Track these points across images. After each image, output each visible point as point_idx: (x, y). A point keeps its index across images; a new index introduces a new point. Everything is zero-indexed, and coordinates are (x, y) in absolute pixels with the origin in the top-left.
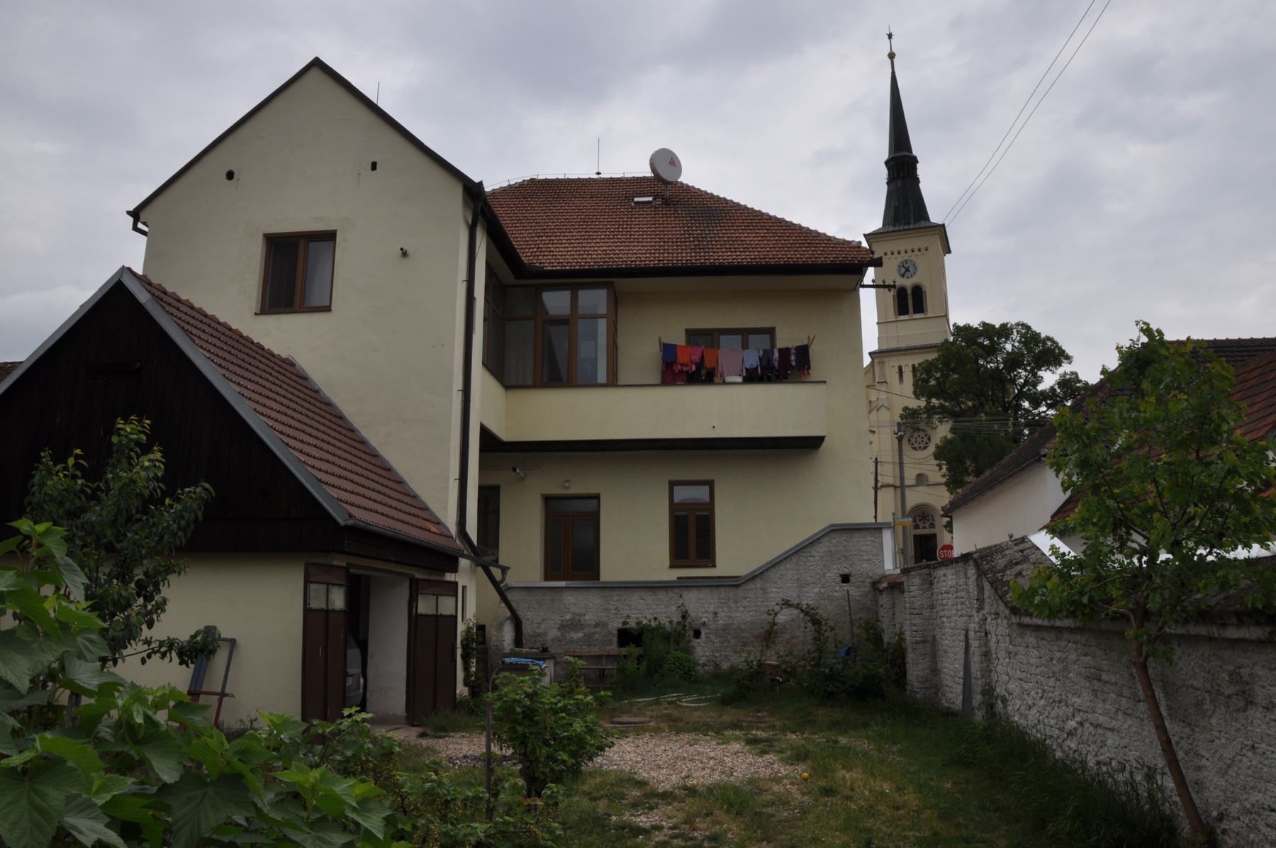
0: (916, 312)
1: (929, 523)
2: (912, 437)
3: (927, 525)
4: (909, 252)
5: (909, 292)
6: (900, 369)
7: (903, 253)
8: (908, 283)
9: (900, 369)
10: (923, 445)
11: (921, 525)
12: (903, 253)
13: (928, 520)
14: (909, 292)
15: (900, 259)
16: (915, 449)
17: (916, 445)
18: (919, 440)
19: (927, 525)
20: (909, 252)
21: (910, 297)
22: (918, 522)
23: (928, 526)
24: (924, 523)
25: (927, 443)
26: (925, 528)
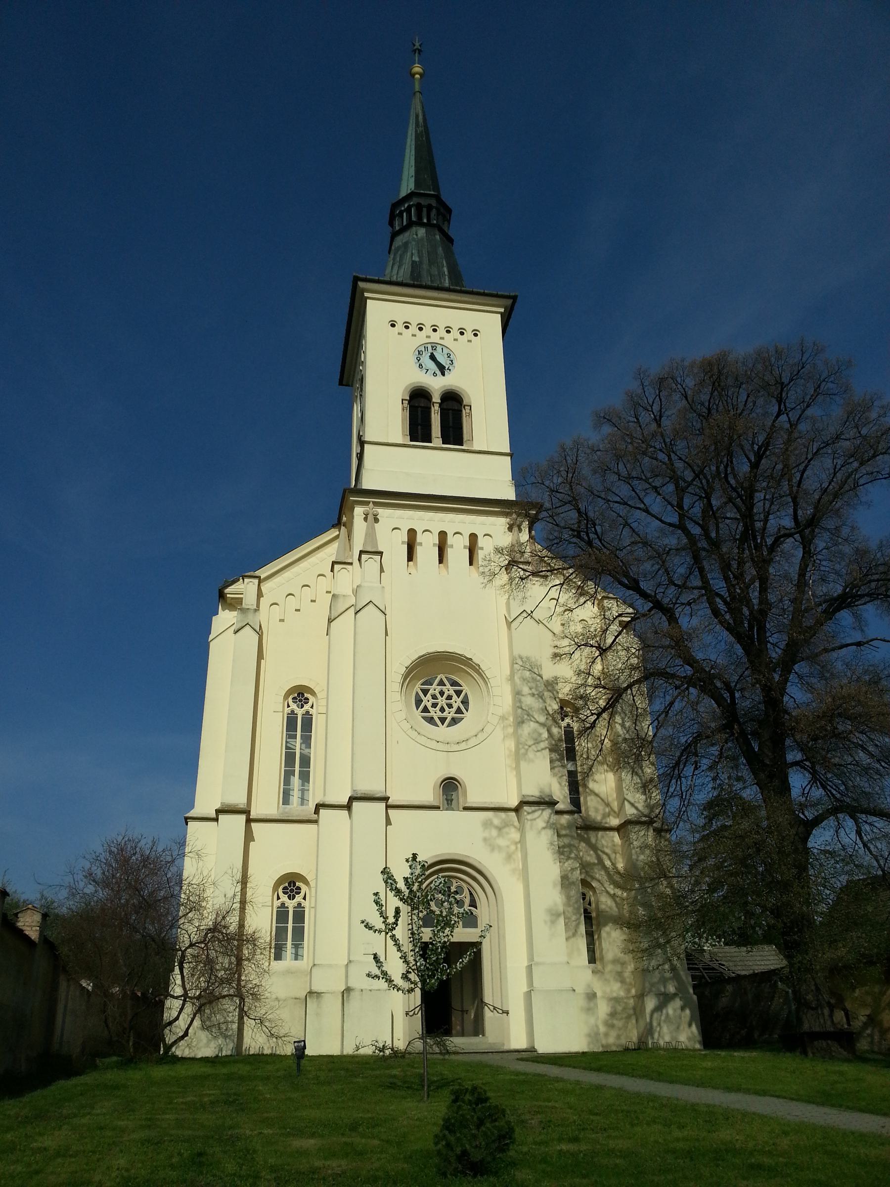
2: (425, 692)
4: (441, 332)
5: (436, 399)
6: (412, 533)
7: (428, 330)
8: (436, 385)
9: (412, 533)
10: (450, 714)
12: (428, 330)
13: (460, 903)
14: (436, 399)
15: (422, 338)
16: (431, 720)
17: (435, 713)
18: (442, 701)
20: (441, 332)
25: (459, 711)
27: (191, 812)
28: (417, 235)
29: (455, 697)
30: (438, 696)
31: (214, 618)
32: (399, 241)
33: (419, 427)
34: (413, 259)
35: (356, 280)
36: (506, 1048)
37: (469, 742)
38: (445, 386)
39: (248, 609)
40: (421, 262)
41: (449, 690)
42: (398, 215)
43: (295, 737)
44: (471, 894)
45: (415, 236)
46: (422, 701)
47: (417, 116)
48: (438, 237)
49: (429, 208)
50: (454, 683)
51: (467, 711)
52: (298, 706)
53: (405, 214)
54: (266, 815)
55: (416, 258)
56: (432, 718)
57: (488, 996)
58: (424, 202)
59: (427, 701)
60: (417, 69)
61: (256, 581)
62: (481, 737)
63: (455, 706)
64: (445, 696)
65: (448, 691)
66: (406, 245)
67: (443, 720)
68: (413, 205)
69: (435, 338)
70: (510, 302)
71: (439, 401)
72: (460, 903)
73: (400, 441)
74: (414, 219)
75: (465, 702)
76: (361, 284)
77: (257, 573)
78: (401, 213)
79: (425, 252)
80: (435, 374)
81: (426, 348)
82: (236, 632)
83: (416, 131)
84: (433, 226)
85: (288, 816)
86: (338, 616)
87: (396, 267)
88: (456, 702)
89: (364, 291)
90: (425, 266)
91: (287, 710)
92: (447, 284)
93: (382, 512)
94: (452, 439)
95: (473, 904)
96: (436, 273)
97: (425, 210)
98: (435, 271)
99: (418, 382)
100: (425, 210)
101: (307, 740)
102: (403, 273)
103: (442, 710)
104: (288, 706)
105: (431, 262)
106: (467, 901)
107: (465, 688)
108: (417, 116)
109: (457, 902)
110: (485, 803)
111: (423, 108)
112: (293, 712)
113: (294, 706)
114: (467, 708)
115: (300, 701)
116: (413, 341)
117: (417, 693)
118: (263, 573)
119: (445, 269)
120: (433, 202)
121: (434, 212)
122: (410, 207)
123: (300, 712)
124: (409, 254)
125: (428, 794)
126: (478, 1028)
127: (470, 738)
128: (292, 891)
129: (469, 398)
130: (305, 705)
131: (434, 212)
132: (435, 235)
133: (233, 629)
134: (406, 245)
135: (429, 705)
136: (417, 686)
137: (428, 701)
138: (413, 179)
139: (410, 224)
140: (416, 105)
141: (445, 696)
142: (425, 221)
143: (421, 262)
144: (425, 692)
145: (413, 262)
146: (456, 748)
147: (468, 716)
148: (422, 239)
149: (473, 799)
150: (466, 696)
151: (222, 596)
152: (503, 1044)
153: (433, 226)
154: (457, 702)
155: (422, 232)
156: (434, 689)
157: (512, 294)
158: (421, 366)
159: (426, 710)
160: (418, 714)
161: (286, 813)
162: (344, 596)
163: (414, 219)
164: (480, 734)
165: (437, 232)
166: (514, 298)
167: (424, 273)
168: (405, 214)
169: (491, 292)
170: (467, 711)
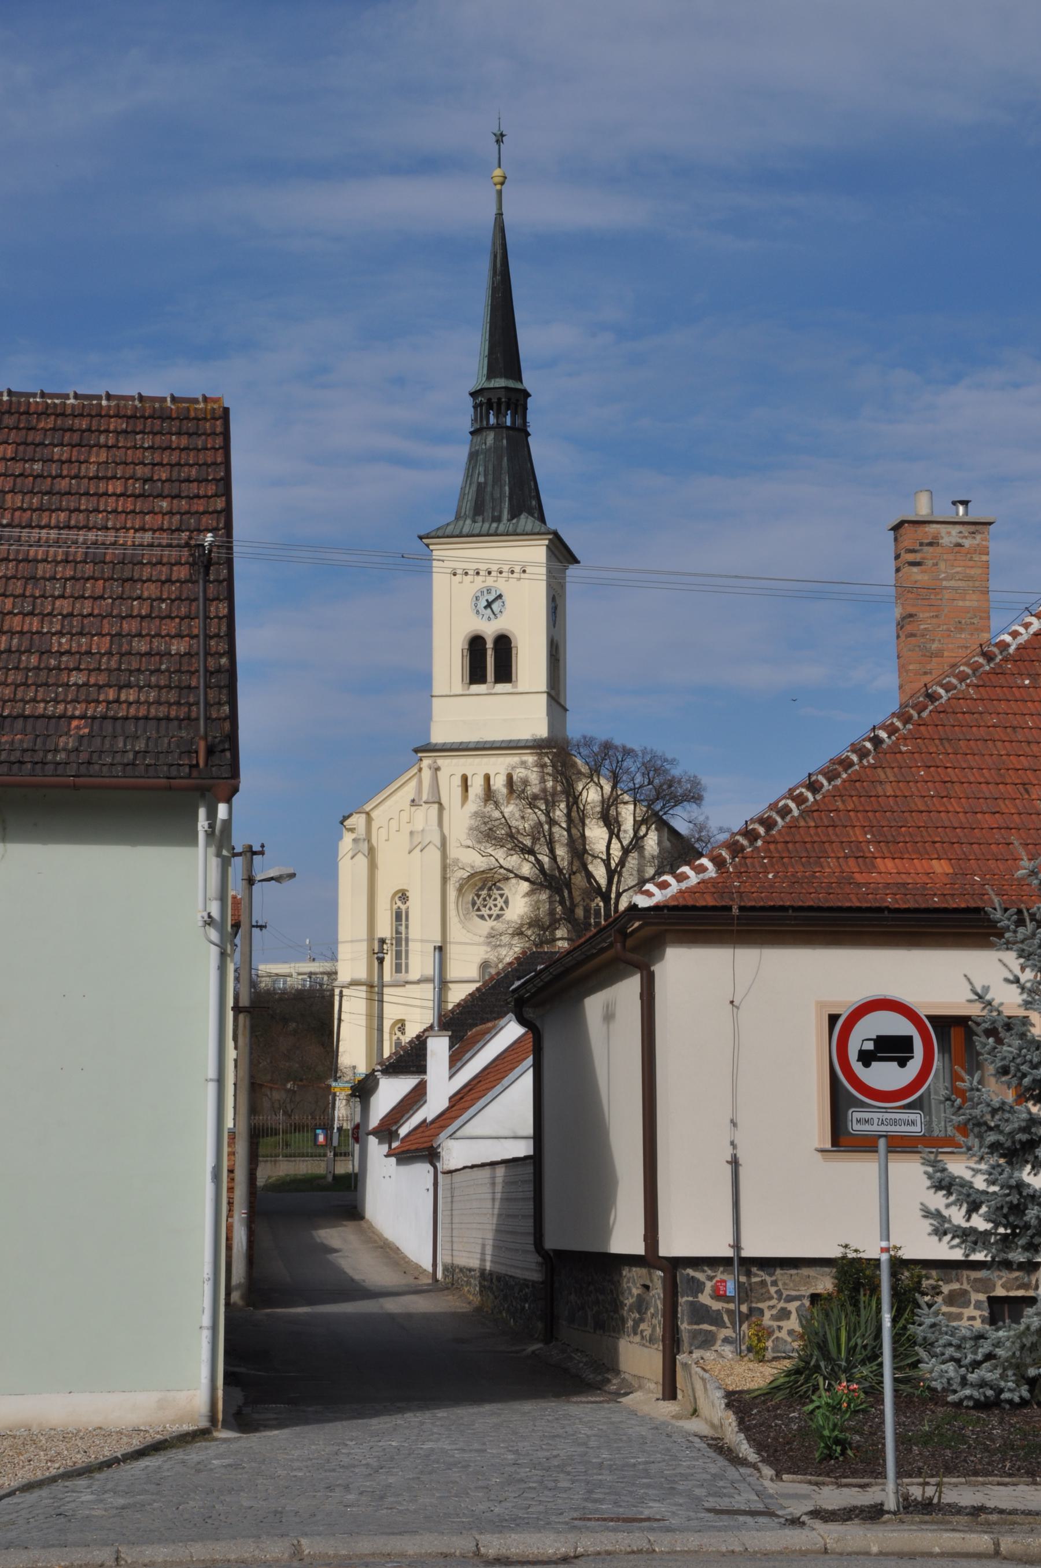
5: (490, 645)
8: (489, 630)
15: (479, 582)
31: (340, 843)
40: (486, 483)
43: (401, 925)
55: (482, 479)
61: (364, 816)
64: (493, 898)
69: (490, 581)
73: (461, 693)
75: (506, 902)
79: (491, 467)
80: (489, 619)
82: (352, 858)
90: (489, 489)
91: (395, 907)
93: (440, 762)
98: (497, 495)
105: (497, 480)
107: (506, 892)
112: (399, 908)
113: (399, 904)
116: (472, 586)
119: (507, 488)
123: (403, 907)
132: (502, 440)
133: (350, 854)
145: (479, 484)
150: (507, 897)
167: (488, 498)
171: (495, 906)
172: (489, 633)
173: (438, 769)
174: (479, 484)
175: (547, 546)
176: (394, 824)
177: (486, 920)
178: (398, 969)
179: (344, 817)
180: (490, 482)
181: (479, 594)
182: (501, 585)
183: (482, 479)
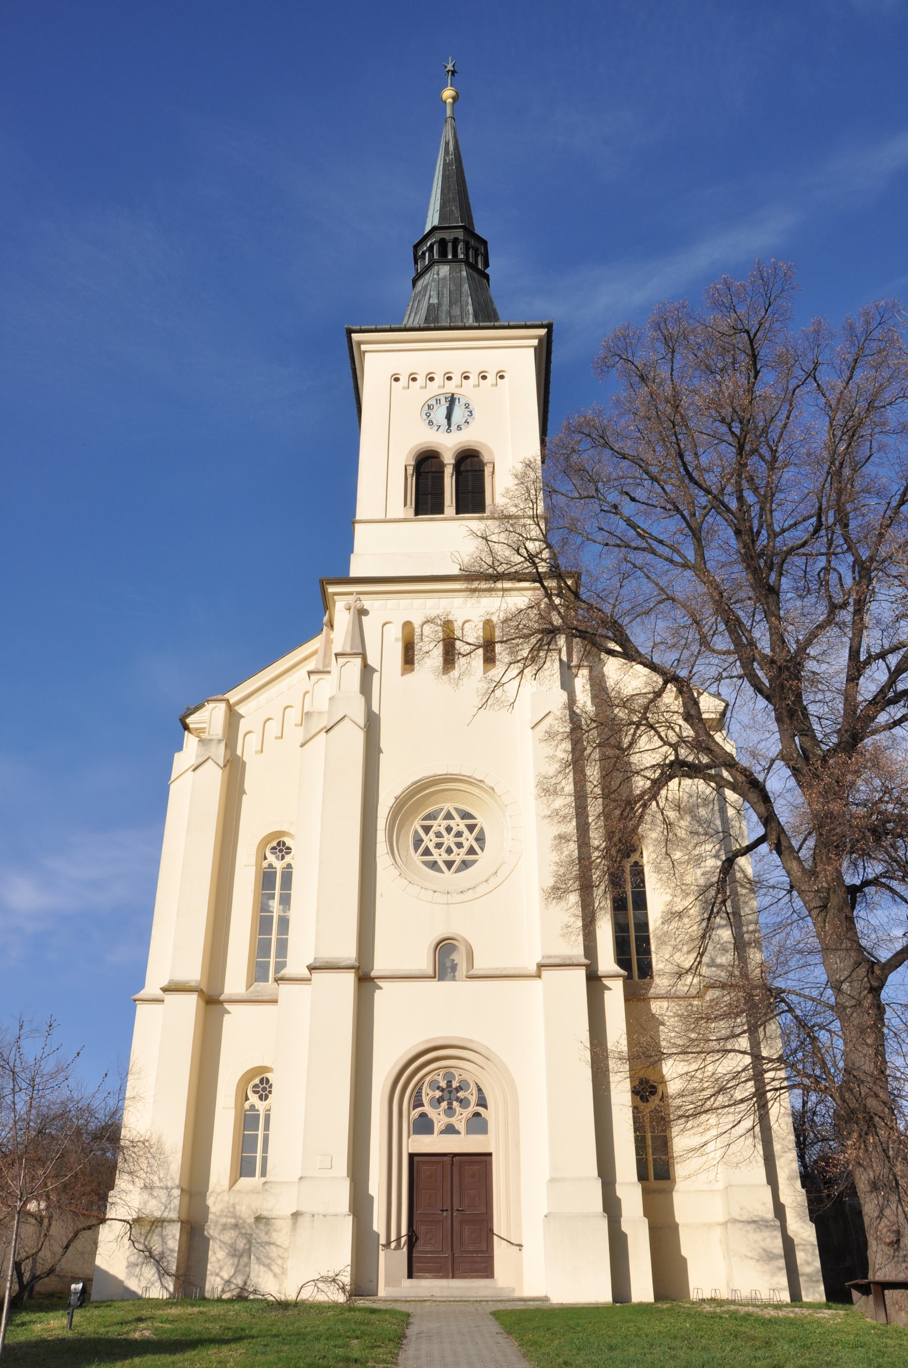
0: (461, 508)
1: (468, 1112)
2: (427, 829)
3: (460, 1119)
5: (449, 459)
7: (439, 379)
11: (439, 1118)
13: (464, 1103)
14: (449, 459)
15: (434, 389)
17: (439, 856)
18: (449, 840)
19: (460, 1119)
21: (449, 471)
22: (427, 1109)
23: (461, 1126)
24: (450, 1111)
25: (471, 851)
26: (450, 1130)
27: (141, 992)
28: (438, 274)
29: (466, 832)
30: (444, 833)
31: (176, 755)
32: (420, 284)
33: (429, 497)
34: (431, 302)
35: (350, 332)
36: (517, 1294)
37: (478, 889)
38: (460, 443)
39: (210, 740)
40: (439, 304)
41: (459, 824)
42: (420, 257)
44: (480, 1090)
45: (436, 276)
46: (422, 841)
47: (447, 144)
48: (464, 273)
49: (455, 241)
50: (466, 815)
51: (482, 849)
52: (277, 858)
53: (427, 254)
54: (231, 994)
55: (434, 301)
56: (435, 862)
57: (499, 1225)
58: (448, 236)
59: (429, 841)
60: (448, 94)
62: (494, 882)
63: (466, 845)
64: (453, 832)
65: (458, 825)
66: (425, 288)
67: (449, 864)
68: (435, 242)
69: (450, 387)
70: (543, 332)
71: (453, 461)
72: (464, 1103)
74: (436, 257)
75: (480, 839)
76: (355, 337)
77: (227, 696)
78: (424, 253)
79: (446, 292)
81: (438, 401)
83: (445, 160)
84: (461, 261)
85: (258, 996)
86: (311, 738)
87: (413, 314)
88: (467, 840)
89: (359, 343)
90: (445, 308)
92: (471, 321)
94: (470, 507)
95: (482, 1103)
96: (459, 313)
97: (450, 245)
99: (426, 443)
100: (450, 245)
101: (286, 901)
102: (419, 319)
103: (449, 851)
104: (265, 858)
106: (473, 1099)
107: (481, 821)
108: (447, 144)
109: (460, 1101)
110: (497, 969)
111: (455, 134)
112: (270, 866)
113: (271, 858)
114: (481, 846)
115: (281, 851)
117: (416, 832)
118: (234, 696)
119: (470, 308)
120: (460, 234)
121: (461, 247)
122: (432, 246)
123: (279, 865)
124: (427, 297)
125: (424, 962)
126: (486, 1269)
127: (477, 885)
128: (264, 1089)
129: (491, 453)
130: (286, 856)
131: (461, 247)
132: (461, 271)
134: (425, 288)
135: (431, 846)
136: (416, 822)
137: (431, 840)
138: (438, 213)
139: (432, 263)
140: (448, 134)
141: (453, 832)
142: (450, 257)
143: (439, 304)
144: (427, 829)
146: (460, 898)
147: (483, 858)
148: (444, 278)
149: (481, 965)
150: (482, 831)
151: (186, 727)
152: (514, 1290)
153: (461, 261)
154: (469, 839)
155: (444, 270)
156: (439, 825)
157: (545, 322)
158: (431, 423)
159: (427, 852)
160: (417, 858)
161: (258, 992)
162: (319, 713)
163: (436, 257)
164: (492, 879)
165: (463, 267)
166: (549, 327)
168: (427, 254)
169: (518, 323)
170: (482, 849)
171: (459, 845)
172: (450, 446)
173: (362, 612)
174: (430, 305)
175: (536, 348)
176: (273, 728)
177: (441, 871)
178: (258, 972)
179: (188, 709)
180: (446, 301)
181: (433, 402)
182: (466, 391)
183: (434, 301)
